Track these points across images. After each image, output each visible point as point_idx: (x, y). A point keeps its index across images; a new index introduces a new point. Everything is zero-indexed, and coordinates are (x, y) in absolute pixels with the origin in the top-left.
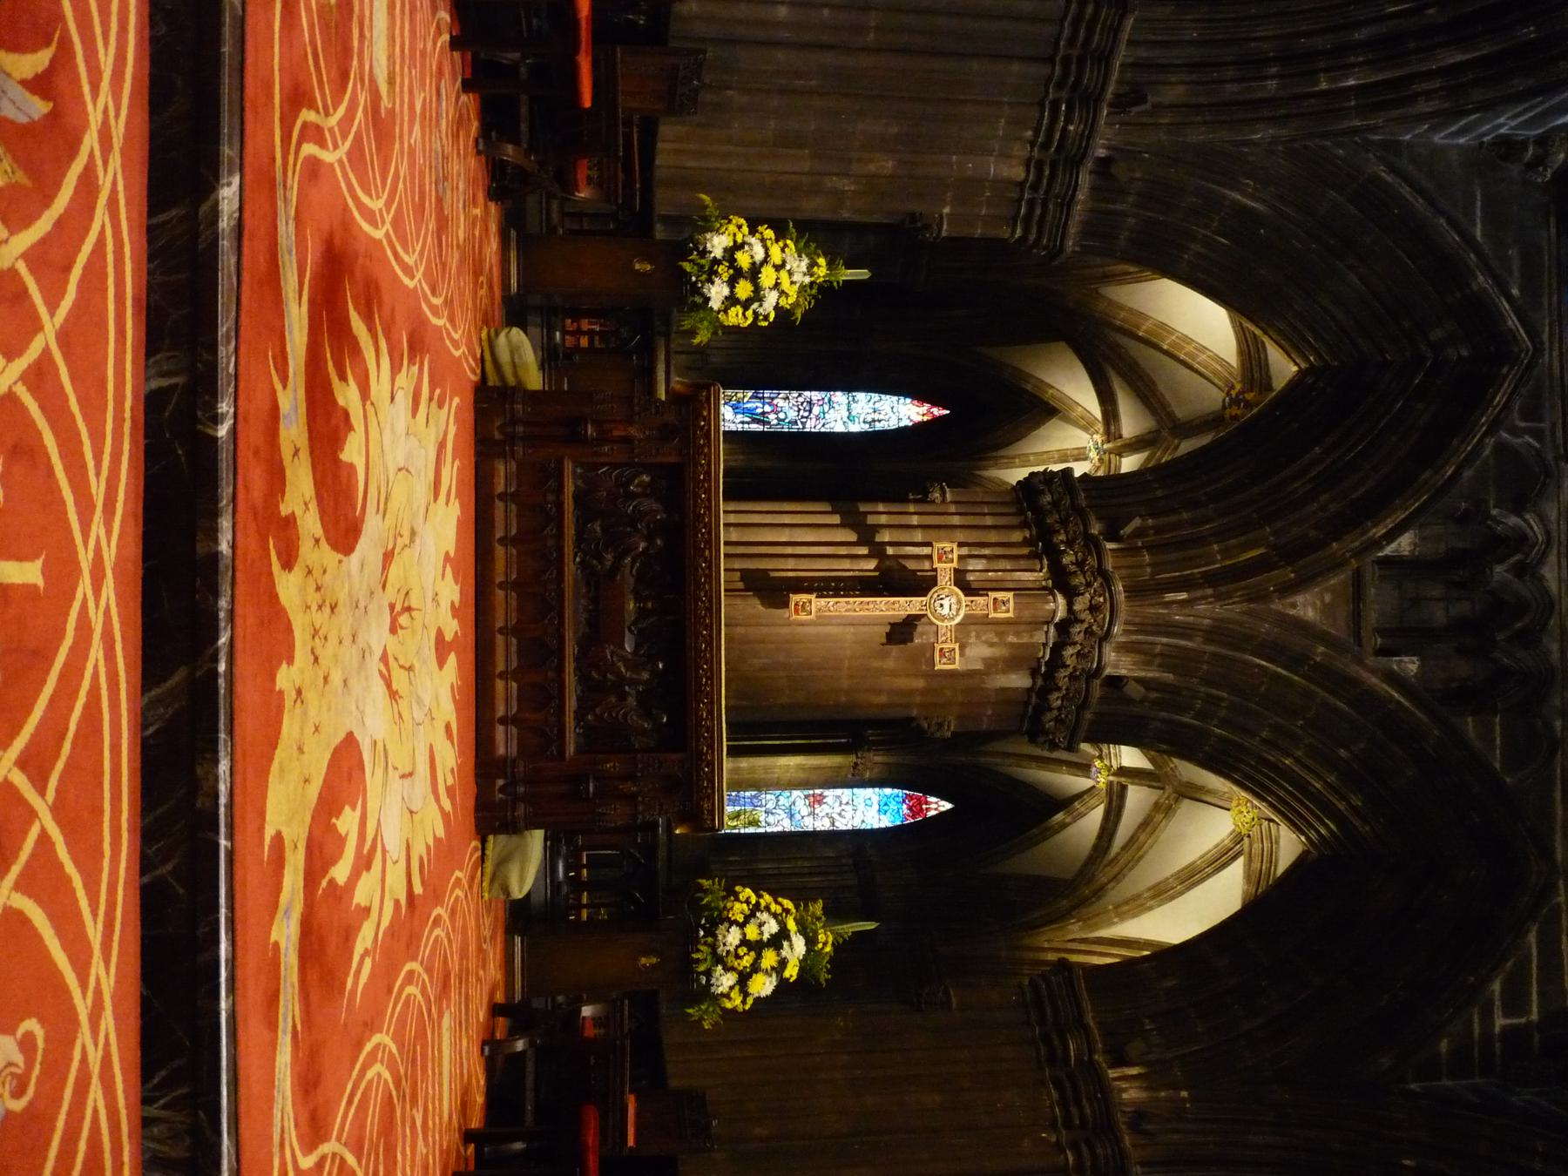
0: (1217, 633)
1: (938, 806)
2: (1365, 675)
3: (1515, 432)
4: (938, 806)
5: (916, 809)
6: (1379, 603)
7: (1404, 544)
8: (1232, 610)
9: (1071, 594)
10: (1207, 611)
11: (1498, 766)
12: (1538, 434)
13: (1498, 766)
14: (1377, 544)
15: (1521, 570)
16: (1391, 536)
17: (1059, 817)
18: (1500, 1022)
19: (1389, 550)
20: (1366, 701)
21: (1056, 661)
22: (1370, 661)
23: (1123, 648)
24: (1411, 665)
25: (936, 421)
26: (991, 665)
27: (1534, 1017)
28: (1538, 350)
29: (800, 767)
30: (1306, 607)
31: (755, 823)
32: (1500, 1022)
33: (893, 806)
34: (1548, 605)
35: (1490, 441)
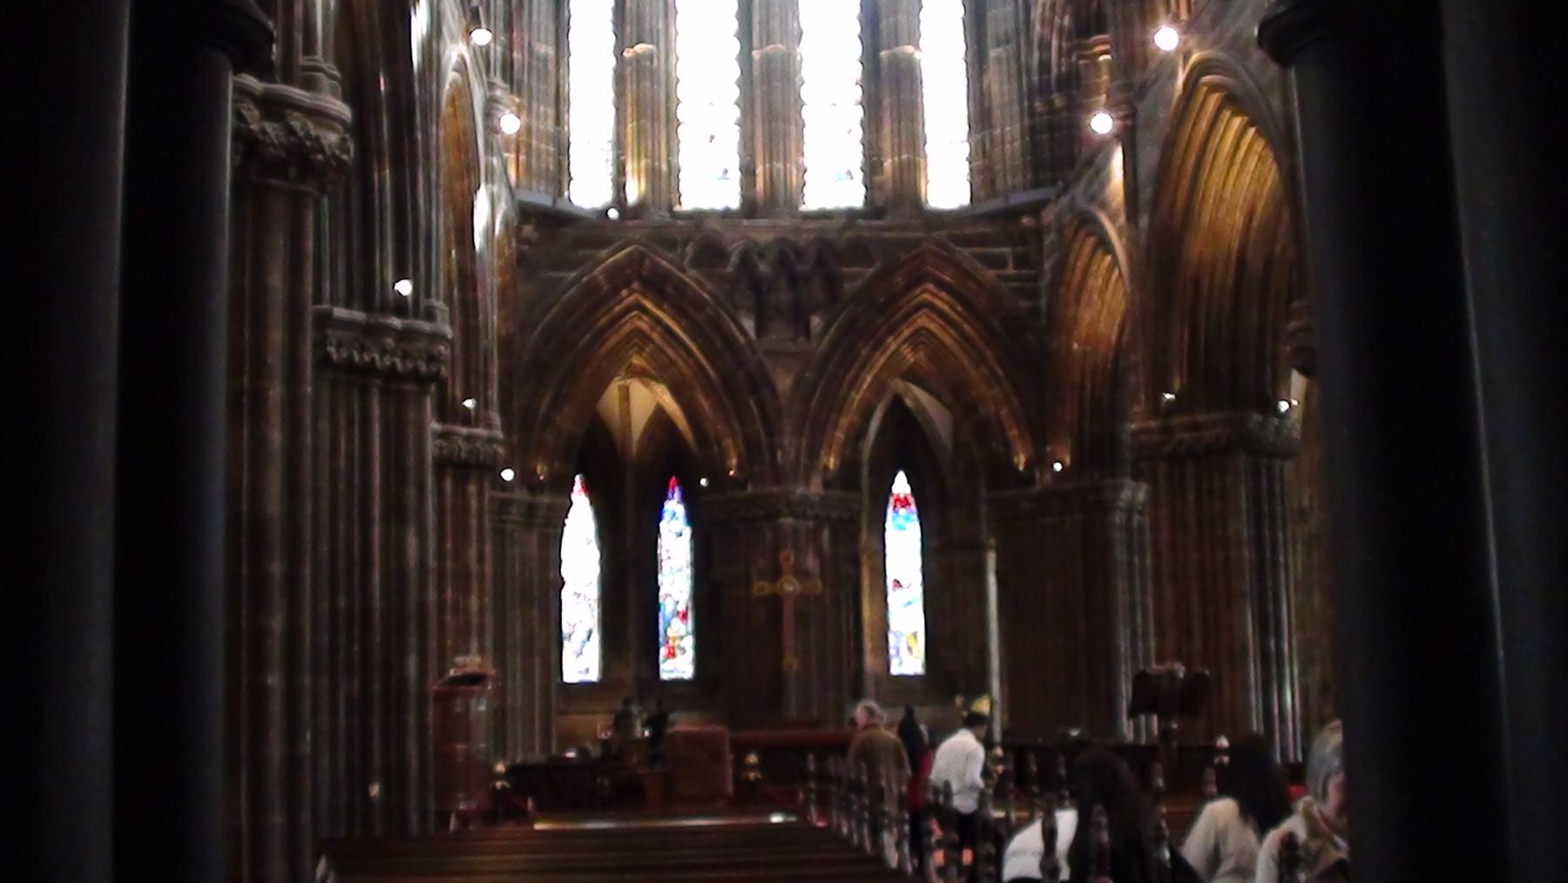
0: (798, 433)
1: (901, 486)
2: (822, 347)
3: (682, 257)
4: (901, 486)
5: (904, 503)
6: (779, 334)
7: (749, 324)
8: (787, 427)
9: (778, 515)
10: (787, 440)
11: (871, 271)
12: (685, 244)
13: (871, 271)
14: (749, 341)
15: (761, 255)
16: (744, 332)
17: (908, 402)
18: (1010, 271)
19: (752, 334)
20: (834, 345)
21: (816, 518)
22: (814, 344)
23: (808, 482)
24: (816, 321)
25: (588, 488)
26: (819, 553)
27: (1006, 250)
28: (636, 242)
29: (872, 601)
30: (784, 382)
31: (915, 635)
32: (1010, 271)
33: (901, 521)
34: (782, 241)
35: (693, 272)
